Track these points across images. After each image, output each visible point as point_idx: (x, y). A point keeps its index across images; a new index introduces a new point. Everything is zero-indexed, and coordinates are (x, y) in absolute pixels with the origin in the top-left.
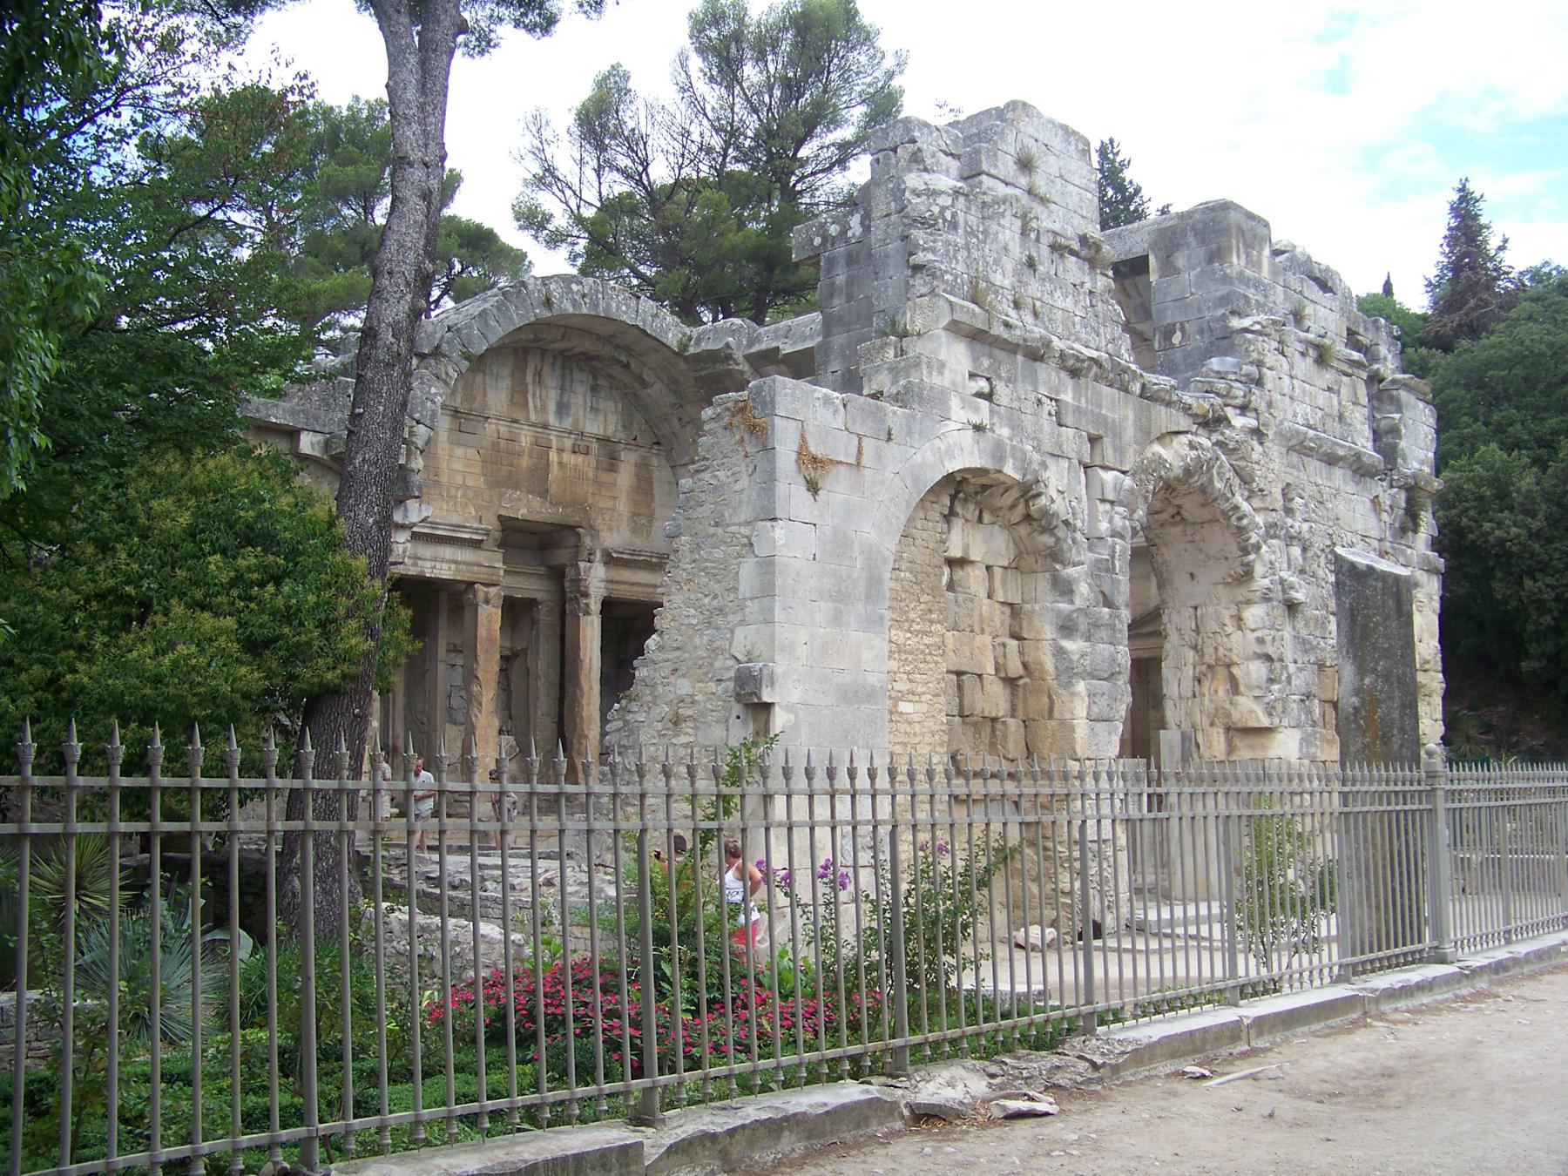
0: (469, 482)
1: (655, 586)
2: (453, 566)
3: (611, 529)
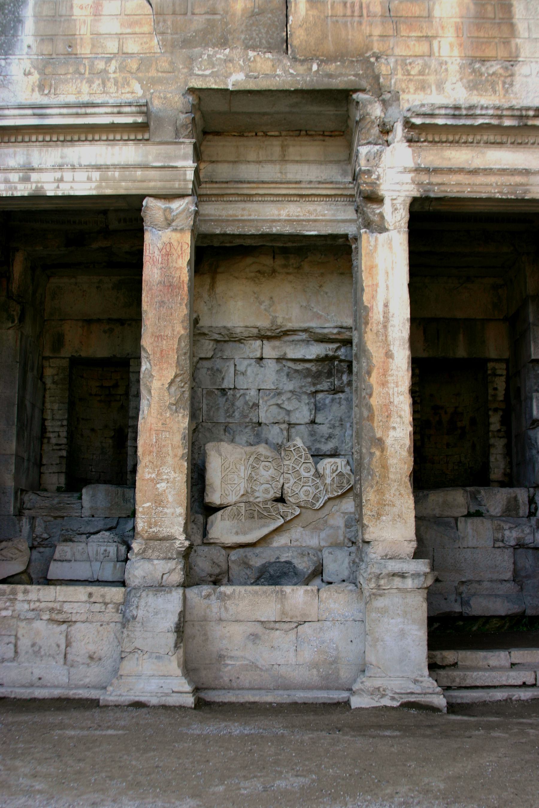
0: (132, 47)
1: (527, 172)
2: (96, 175)
3: (423, 87)
